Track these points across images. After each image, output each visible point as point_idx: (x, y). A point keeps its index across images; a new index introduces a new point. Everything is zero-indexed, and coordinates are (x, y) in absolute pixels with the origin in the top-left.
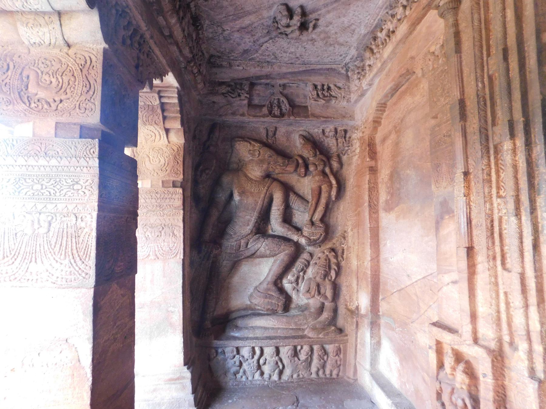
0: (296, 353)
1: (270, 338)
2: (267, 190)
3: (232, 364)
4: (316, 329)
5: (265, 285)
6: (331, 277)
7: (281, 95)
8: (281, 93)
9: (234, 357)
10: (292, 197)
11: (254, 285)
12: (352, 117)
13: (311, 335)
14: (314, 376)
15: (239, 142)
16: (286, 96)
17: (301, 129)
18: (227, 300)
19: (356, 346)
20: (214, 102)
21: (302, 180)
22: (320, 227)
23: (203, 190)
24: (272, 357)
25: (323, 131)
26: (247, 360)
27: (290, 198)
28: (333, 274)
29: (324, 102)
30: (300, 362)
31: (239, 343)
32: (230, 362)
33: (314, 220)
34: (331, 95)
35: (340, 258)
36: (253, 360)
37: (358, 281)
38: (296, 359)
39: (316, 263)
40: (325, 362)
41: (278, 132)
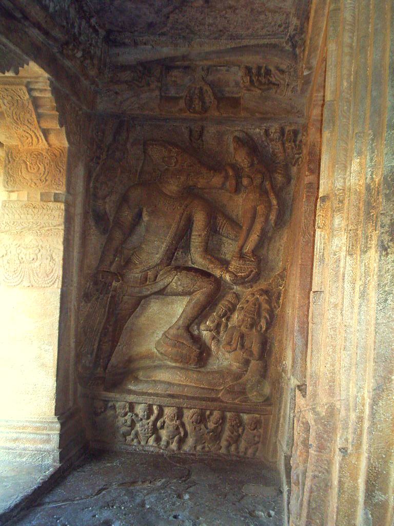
1: (172, 396)
2: (184, 210)
3: (122, 422)
6: (261, 328)
9: (126, 414)
13: (225, 400)
14: (223, 451)
15: (151, 146)
16: (212, 85)
21: (236, 198)
24: (172, 420)
26: (141, 420)
28: (263, 324)
29: (259, 91)
31: (131, 398)
32: (121, 420)
34: (270, 83)
38: (203, 426)
39: (242, 308)
40: (239, 436)
41: (205, 132)
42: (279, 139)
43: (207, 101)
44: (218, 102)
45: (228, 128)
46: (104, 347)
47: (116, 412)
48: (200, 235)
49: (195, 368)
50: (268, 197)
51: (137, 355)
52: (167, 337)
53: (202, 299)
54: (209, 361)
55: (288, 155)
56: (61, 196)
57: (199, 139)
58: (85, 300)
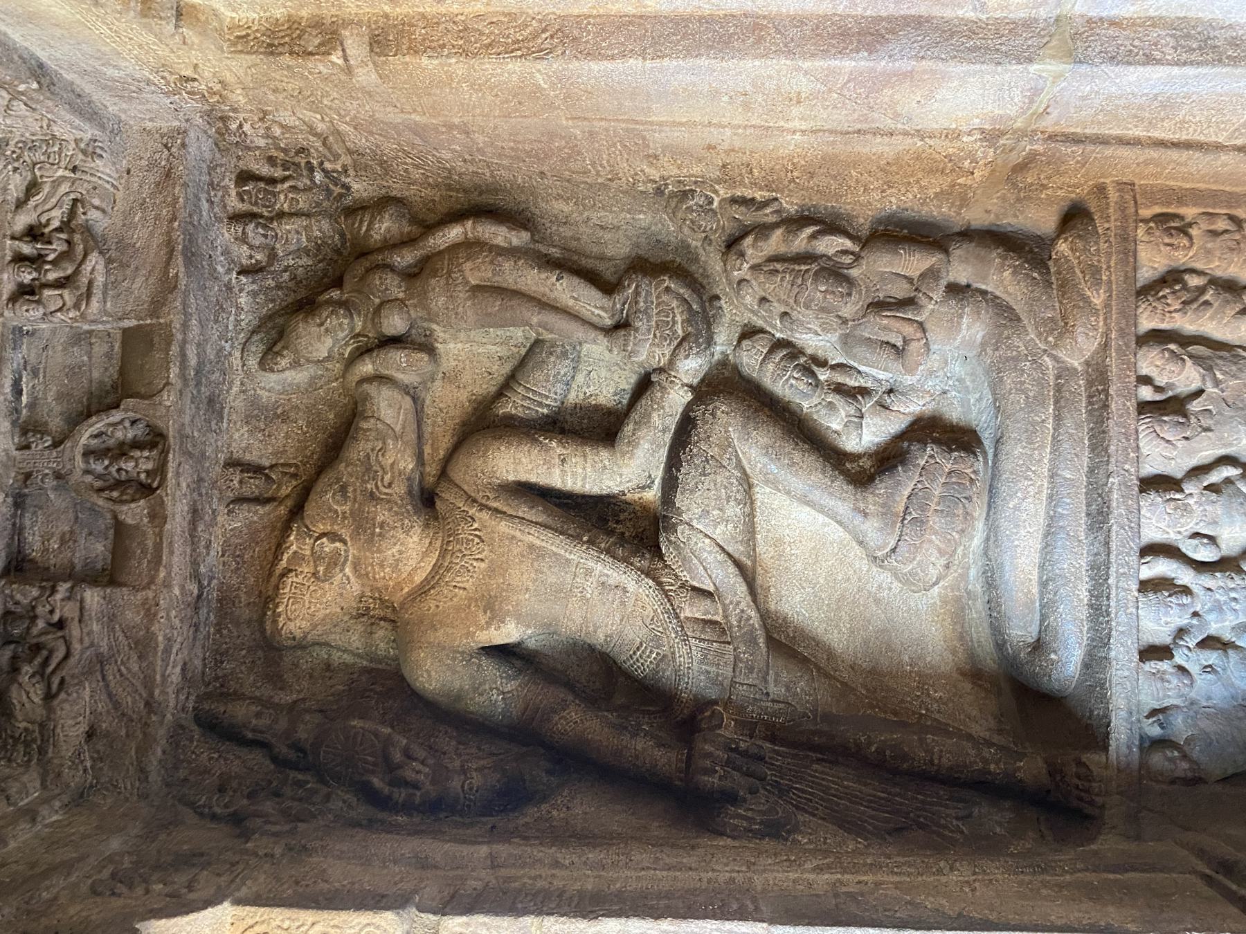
0: (1171, 407)
1: (1099, 517)
2: (483, 507)
4: (1064, 318)
5: (871, 528)
6: (845, 252)
7: (68, 444)
8: (56, 444)
9: (1181, 669)
10: (513, 406)
11: (864, 565)
12: (173, 141)
15: (281, 620)
17: (236, 361)
18: (925, 679)
20: (90, 735)
21: (448, 364)
23: (473, 772)
24: (1187, 509)
25: (243, 272)
26: (1195, 614)
27: (520, 412)
28: (831, 245)
29: (94, 260)
31: (1122, 653)
33: (608, 322)
34: (65, 226)
38: (1195, 406)
41: (252, 457)
42: (265, 227)
43: (130, 435)
44: (131, 397)
45: (235, 390)
46: (944, 760)
47: (1177, 707)
48: (563, 461)
49: (985, 458)
50: (441, 252)
51: (954, 652)
52: (894, 550)
54: (955, 421)
55: (318, 204)
57: (268, 477)
58: (789, 832)
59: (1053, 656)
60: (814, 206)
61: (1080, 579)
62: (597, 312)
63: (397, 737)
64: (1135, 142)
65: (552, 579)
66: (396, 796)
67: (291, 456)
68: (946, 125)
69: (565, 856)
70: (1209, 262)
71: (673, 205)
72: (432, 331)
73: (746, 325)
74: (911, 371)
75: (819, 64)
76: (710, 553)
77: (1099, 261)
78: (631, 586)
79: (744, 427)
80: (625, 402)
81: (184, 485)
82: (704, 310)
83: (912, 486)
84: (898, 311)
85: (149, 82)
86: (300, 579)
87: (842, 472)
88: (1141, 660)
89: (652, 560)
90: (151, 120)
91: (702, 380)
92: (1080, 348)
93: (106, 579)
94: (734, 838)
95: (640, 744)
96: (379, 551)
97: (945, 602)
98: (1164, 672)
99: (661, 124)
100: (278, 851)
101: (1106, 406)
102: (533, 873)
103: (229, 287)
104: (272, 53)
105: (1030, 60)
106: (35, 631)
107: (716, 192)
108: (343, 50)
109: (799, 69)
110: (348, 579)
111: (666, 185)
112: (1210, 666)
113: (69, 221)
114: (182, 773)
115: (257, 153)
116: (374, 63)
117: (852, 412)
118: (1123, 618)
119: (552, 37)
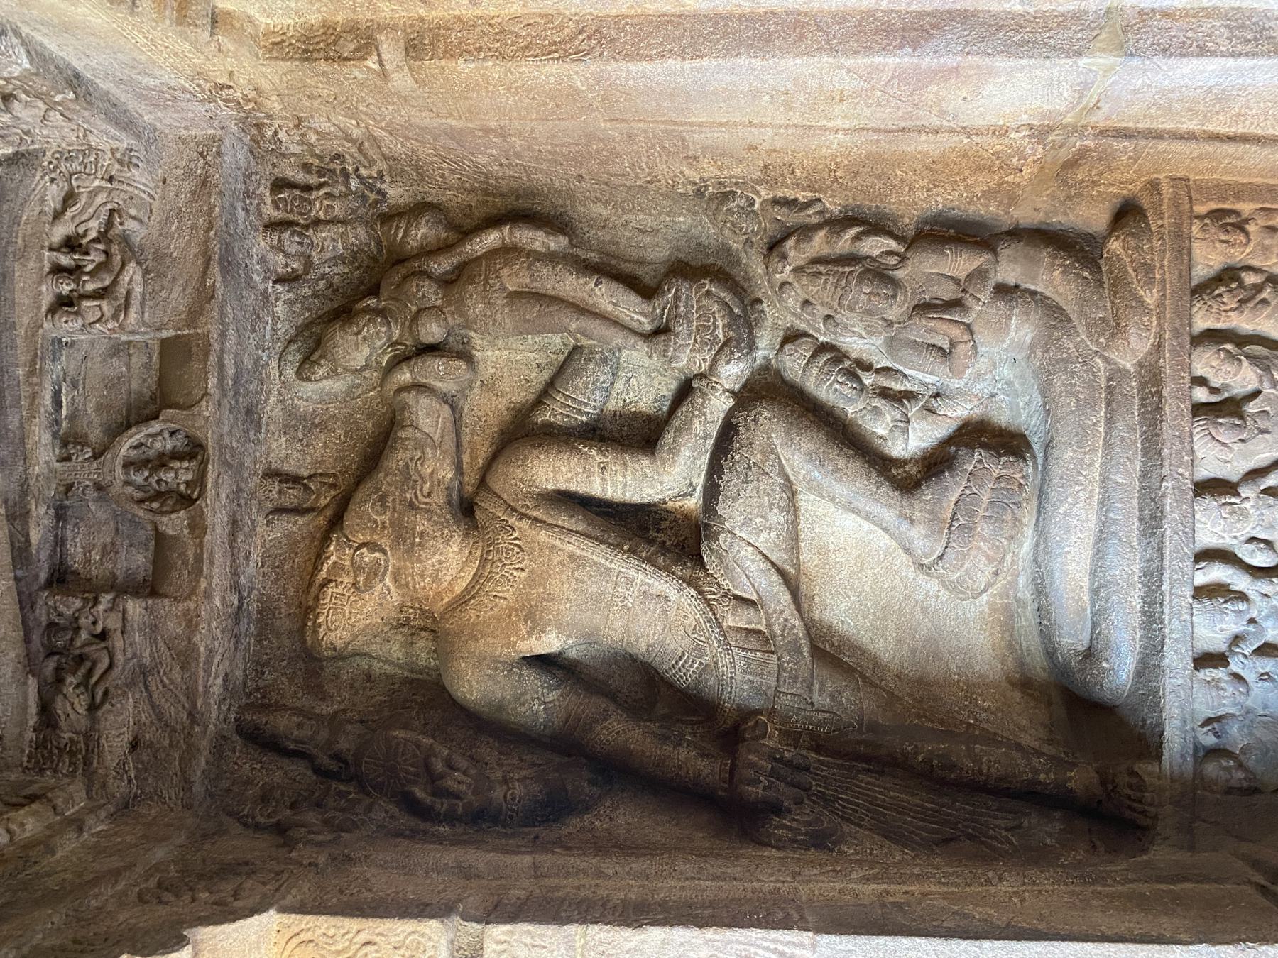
0: (1227, 408)
1: (1152, 522)
2: (523, 516)
4: (1116, 317)
5: (917, 535)
8: (96, 456)
9: (1237, 677)
10: (551, 414)
11: (911, 573)
12: (208, 149)
15: (322, 630)
17: (273, 370)
18: (972, 688)
19: (1215, 137)
20: (134, 745)
21: (486, 372)
22: (677, 297)
23: (515, 784)
24: (1243, 514)
25: (280, 280)
27: (559, 420)
28: (875, 246)
29: (131, 268)
30: (1268, 390)
31: (1176, 660)
34: (103, 237)
35: (811, 216)
36: (1252, 595)
37: (921, 130)
38: (1251, 408)
41: (286, 467)
42: (301, 235)
43: (169, 446)
44: (170, 407)
45: (272, 400)
46: (992, 770)
47: (1233, 715)
49: (1035, 464)
52: (940, 558)
53: (807, 446)
54: (1004, 425)
55: (354, 211)
56: (464, 941)
57: (306, 487)
58: (835, 843)
59: (1104, 664)
60: (858, 207)
61: (1133, 585)
62: (636, 317)
63: (438, 748)
64: (1190, 137)
65: (593, 589)
66: (438, 806)
67: (328, 466)
68: (994, 121)
69: (608, 866)
70: (1267, 259)
71: (714, 207)
72: (470, 338)
73: (788, 329)
74: (958, 374)
75: (864, 61)
76: (753, 561)
77: (1152, 260)
78: (673, 595)
79: (787, 433)
80: (665, 408)
81: (224, 496)
82: (746, 315)
83: (959, 492)
84: (944, 312)
85: (184, 90)
86: (340, 590)
87: (887, 478)
88: (1195, 668)
89: (693, 569)
90: (186, 128)
91: (744, 386)
92: (1132, 350)
93: (147, 591)
94: (779, 849)
95: (683, 754)
96: (419, 561)
97: (993, 609)
98: (1219, 680)
99: (700, 125)
100: (322, 859)
101: (1159, 409)
102: (576, 883)
103: (265, 297)
104: (307, 59)
105: (1080, 54)
106: (78, 643)
107: (757, 193)
108: (379, 55)
109: (841, 67)
110: (388, 589)
111: (706, 186)
112: (1267, 674)
113: (106, 231)
114: (225, 784)
115: (292, 160)
116: (410, 68)
117: (898, 417)
118: (1176, 625)
119: (589, 38)
